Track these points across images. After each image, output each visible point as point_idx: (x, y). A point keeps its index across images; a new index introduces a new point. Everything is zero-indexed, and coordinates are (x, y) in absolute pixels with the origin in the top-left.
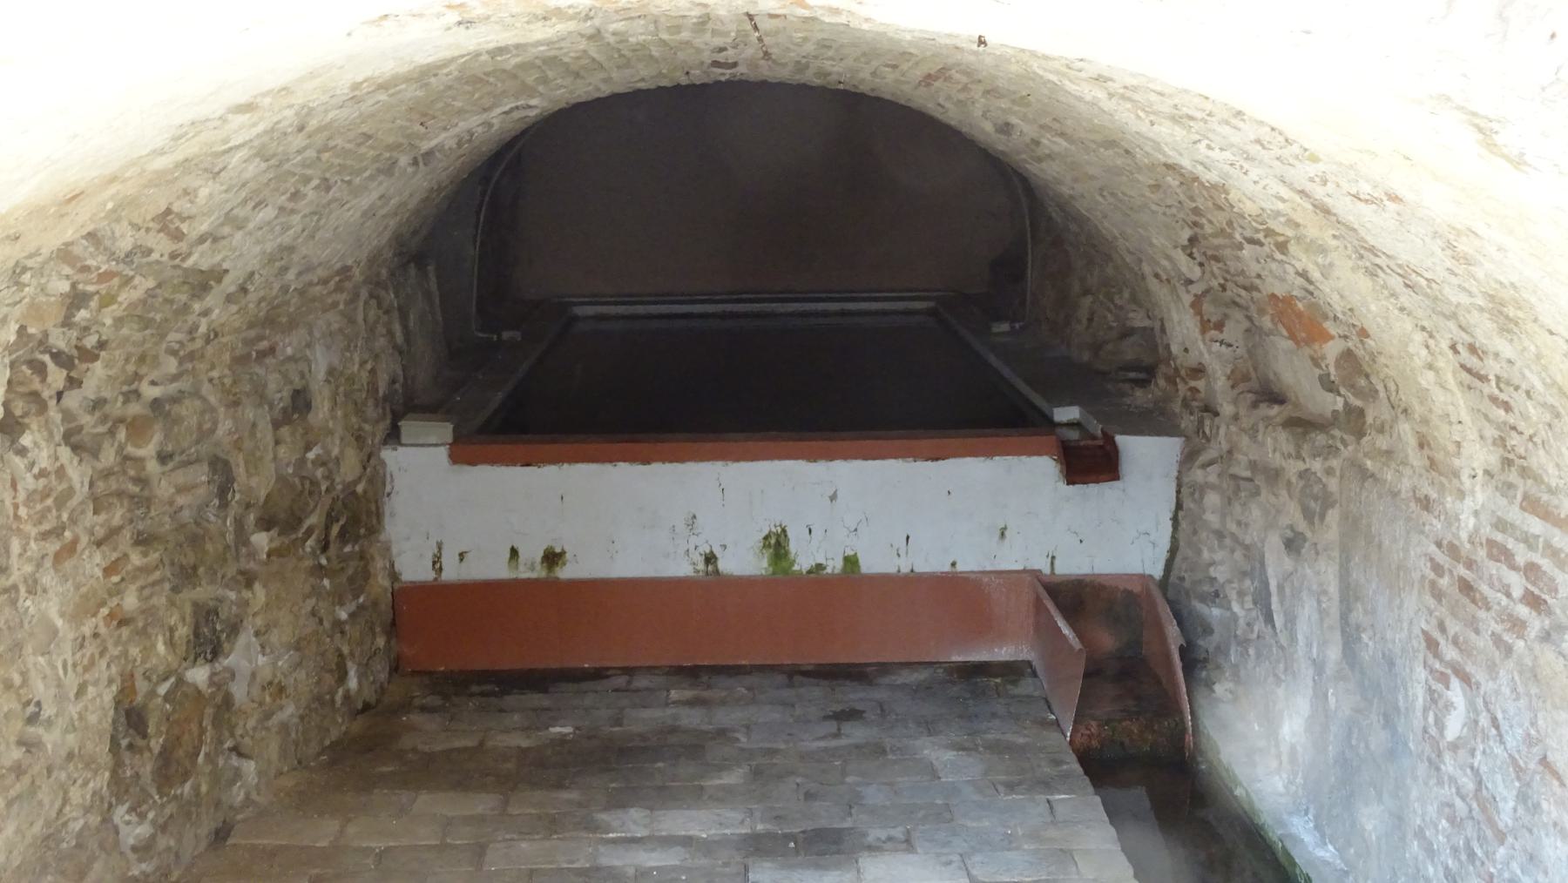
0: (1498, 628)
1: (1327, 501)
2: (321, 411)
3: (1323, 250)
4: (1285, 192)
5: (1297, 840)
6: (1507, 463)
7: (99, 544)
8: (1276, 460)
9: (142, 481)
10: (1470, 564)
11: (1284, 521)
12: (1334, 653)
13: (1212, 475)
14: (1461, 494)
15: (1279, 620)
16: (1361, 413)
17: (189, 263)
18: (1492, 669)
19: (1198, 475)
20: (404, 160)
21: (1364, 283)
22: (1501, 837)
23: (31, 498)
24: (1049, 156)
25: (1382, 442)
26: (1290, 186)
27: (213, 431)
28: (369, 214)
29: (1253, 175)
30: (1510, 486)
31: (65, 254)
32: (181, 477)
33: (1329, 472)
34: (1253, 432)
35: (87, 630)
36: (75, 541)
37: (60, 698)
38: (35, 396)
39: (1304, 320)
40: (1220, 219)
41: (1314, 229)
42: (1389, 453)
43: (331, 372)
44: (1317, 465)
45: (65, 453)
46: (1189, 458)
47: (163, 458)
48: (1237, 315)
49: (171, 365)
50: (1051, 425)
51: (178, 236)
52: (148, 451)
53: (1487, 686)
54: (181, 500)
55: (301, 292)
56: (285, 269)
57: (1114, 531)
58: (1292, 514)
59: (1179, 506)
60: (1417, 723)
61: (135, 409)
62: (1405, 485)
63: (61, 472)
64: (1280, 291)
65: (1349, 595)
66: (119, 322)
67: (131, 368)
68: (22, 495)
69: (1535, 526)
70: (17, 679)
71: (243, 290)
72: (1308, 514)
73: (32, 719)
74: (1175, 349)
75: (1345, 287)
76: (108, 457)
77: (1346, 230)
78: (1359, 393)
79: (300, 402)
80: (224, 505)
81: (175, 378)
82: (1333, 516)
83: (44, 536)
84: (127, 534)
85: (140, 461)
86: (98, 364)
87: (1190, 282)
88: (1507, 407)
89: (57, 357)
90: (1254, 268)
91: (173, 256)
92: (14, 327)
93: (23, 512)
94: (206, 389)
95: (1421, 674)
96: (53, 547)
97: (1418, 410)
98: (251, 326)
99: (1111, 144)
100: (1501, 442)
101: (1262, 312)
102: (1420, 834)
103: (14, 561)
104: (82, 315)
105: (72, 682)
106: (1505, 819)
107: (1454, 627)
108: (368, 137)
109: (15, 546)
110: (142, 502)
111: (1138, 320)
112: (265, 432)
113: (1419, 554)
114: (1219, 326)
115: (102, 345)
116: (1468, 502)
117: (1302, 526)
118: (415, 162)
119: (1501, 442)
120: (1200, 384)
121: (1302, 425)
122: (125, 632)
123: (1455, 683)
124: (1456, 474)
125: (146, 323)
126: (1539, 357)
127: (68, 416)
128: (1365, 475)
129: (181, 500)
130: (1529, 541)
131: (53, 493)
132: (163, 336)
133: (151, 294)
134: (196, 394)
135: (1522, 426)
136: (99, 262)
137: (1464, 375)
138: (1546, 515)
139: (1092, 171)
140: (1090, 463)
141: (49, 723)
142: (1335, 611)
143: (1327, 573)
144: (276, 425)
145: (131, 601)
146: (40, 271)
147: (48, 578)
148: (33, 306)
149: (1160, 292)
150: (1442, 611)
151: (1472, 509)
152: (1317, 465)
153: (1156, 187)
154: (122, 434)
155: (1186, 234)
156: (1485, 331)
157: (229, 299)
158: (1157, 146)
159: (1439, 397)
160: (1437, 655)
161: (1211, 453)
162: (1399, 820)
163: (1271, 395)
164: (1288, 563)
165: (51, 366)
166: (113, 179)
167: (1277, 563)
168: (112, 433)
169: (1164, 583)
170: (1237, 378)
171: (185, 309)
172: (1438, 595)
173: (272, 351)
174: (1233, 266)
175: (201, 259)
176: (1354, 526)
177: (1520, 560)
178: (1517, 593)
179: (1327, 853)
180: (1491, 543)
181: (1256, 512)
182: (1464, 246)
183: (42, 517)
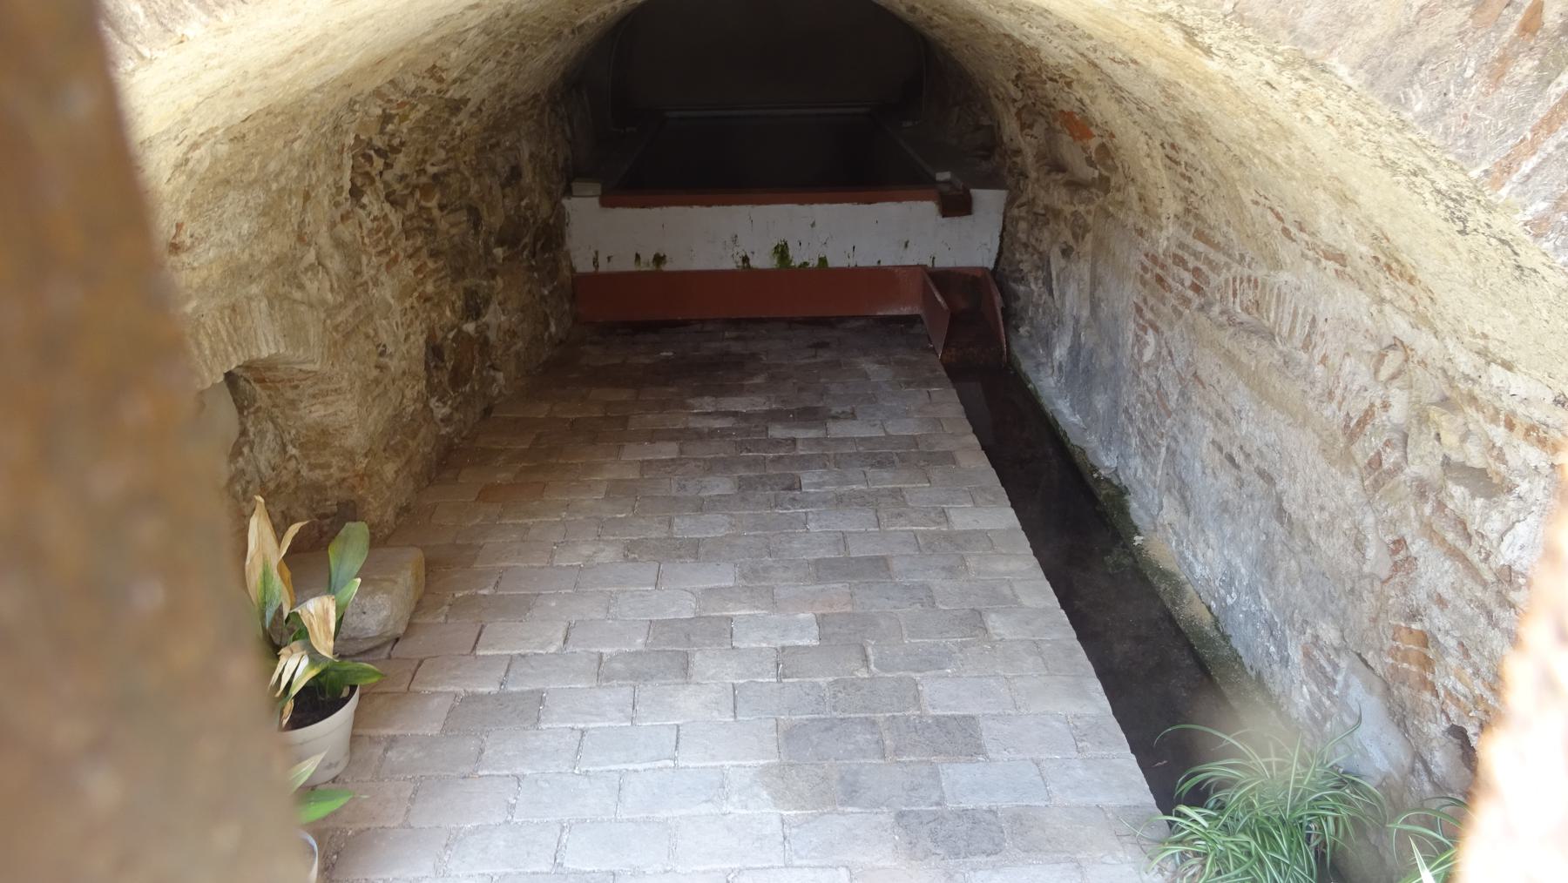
0: (1175, 302)
1: (1086, 229)
2: (527, 178)
3: (1092, 88)
4: (1072, 53)
5: (1060, 412)
6: (1187, 211)
7: (410, 257)
8: (1059, 205)
9: (431, 221)
10: (1163, 267)
11: (1062, 239)
12: (1085, 313)
13: (1023, 212)
14: (1161, 228)
15: (1056, 294)
16: (1108, 180)
17: (448, 95)
18: (1171, 325)
19: (1015, 212)
20: (566, 31)
21: (1114, 107)
22: (1169, 414)
23: (370, 231)
24: (937, 26)
25: (1119, 197)
26: (1076, 50)
27: (468, 191)
28: (548, 62)
29: (1055, 42)
30: (1188, 224)
31: (377, 93)
32: (452, 218)
33: (1089, 212)
34: (1047, 188)
35: (407, 305)
36: (397, 256)
37: (396, 343)
38: (367, 174)
39: (1079, 125)
40: (1034, 66)
41: (1088, 75)
42: (1122, 203)
43: (532, 155)
44: (1082, 208)
45: (387, 206)
46: (1010, 203)
47: (442, 207)
48: (1042, 120)
49: (442, 154)
50: (933, 182)
51: (441, 80)
52: (433, 204)
53: (1167, 334)
54: (454, 231)
55: (512, 110)
56: (502, 97)
57: (969, 244)
58: (1067, 235)
59: (1004, 229)
60: (1128, 352)
61: (424, 179)
62: (1130, 221)
63: (385, 217)
64: (1066, 108)
65: (1095, 281)
66: (411, 130)
67: (420, 157)
68: (365, 232)
69: (1201, 247)
70: (372, 333)
71: (480, 109)
72: (1075, 236)
73: (382, 354)
74: (1005, 139)
75: (1104, 109)
76: (411, 208)
77: (1106, 77)
78: (1107, 168)
79: (516, 173)
80: (477, 233)
81: (444, 162)
82: (1089, 237)
83: (380, 253)
84: (425, 251)
85: (429, 209)
86: (401, 155)
87: (1015, 101)
88: (1190, 180)
89: (378, 151)
90: (1052, 95)
91: (439, 92)
92: (352, 136)
93: (367, 240)
94: (462, 166)
95: (1132, 326)
96: (385, 259)
97: (1140, 179)
98: (485, 130)
99: (973, 21)
100: (1185, 199)
101: (1055, 120)
102: (1126, 411)
103: (364, 268)
104: (390, 127)
105: (401, 333)
106: (1172, 404)
107: (1152, 301)
108: (545, 18)
109: (364, 259)
110: (431, 232)
111: (985, 121)
112: (497, 192)
113: (1135, 260)
114: (1031, 126)
115: (402, 144)
116: (1164, 233)
117: (1071, 242)
118: (573, 32)
119: (1185, 199)
120: (1018, 160)
121: (1075, 185)
122: (428, 305)
123: (1150, 331)
124: (1159, 217)
125: (426, 131)
126: (1210, 154)
127: (386, 184)
128: (1108, 215)
129: (454, 231)
130: (1196, 255)
131: (382, 229)
132: (436, 138)
133: (427, 114)
134: (457, 170)
135: (1197, 191)
136: (397, 97)
137: (1168, 162)
138: (1207, 241)
139: (962, 35)
140: (956, 205)
141: (391, 355)
142: (1087, 289)
143: (1083, 268)
144: (503, 187)
145: (430, 288)
146: (364, 103)
147: (384, 278)
148: (363, 124)
149: (998, 106)
150: (1146, 292)
151: (1166, 236)
152: (1082, 208)
153: (998, 46)
154: (418, 195)
155: (1014, 73)
156: (1181, 137)
157: (472, 115)
158: (1000, 24)
159: (1152, 173)
160: (1141, 316)
161: (1023, 199)
162: (1115, 403)
163: (1059, 167)
164: (1063, 263)
165: (375, 157)
166: (402, 50)
167: (1057, 262)
168: (412, 194)
169: (994, 272)
170: (1040, 156)
171: (448, 122)
172: (1144, 283)
173: (498, 144)
174: (1040, 92)
175: (455, 93)
176: (1100, 243)
177: (1191, 266)
178: (1187, 283)
179: (1076, 419)
180: (1175, 256)
181: (1046, 234)
182: (1172, 91)
183: (378, 242)
